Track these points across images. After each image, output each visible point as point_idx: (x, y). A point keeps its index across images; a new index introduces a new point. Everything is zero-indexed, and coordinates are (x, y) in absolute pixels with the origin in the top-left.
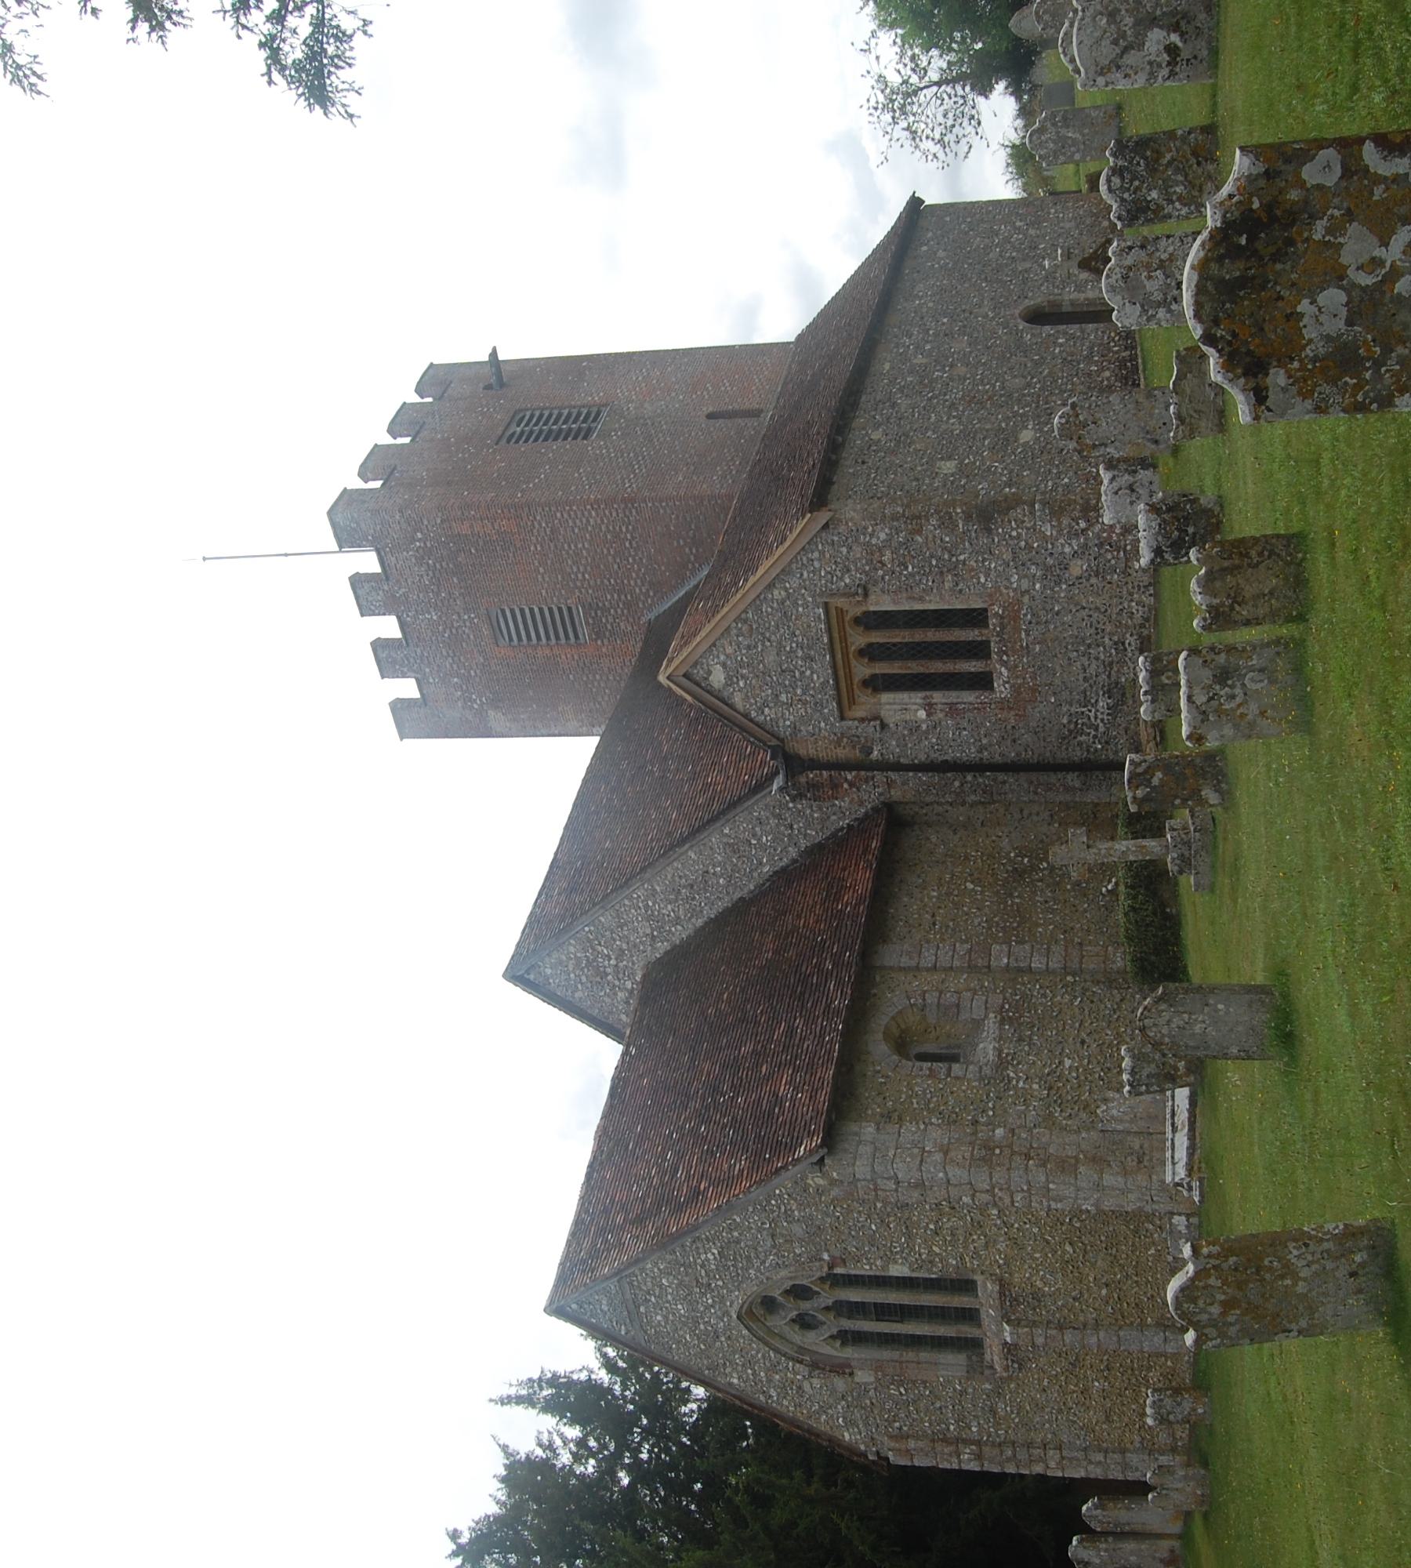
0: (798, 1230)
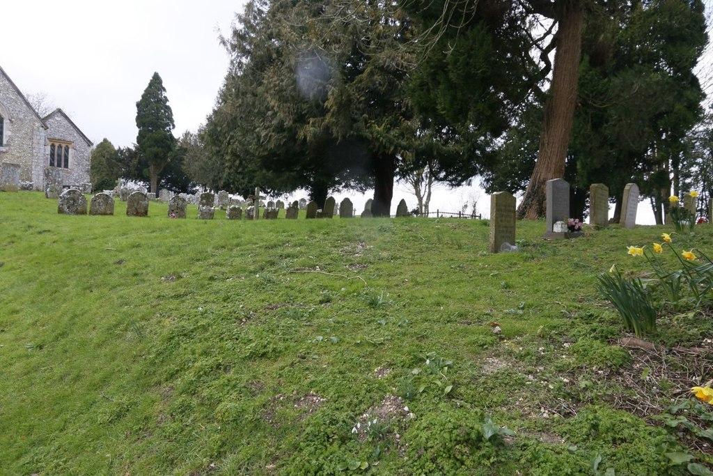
0: (21, 116)
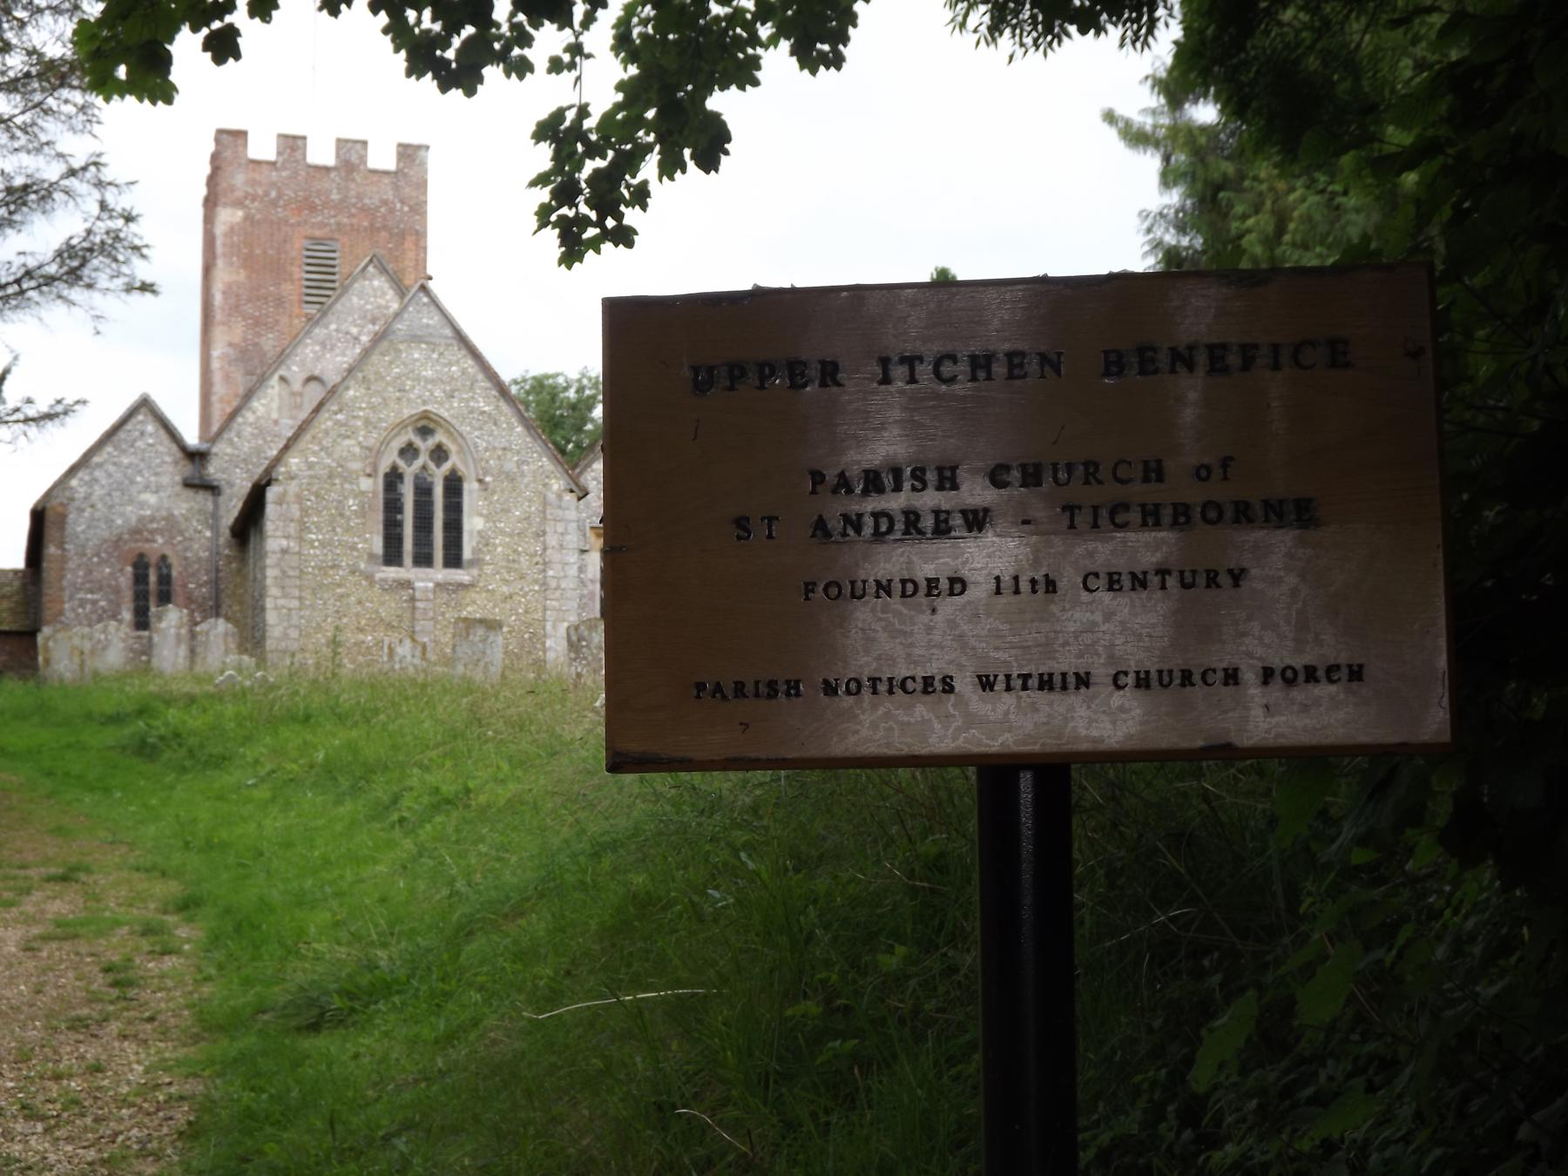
0: (510, 466)
